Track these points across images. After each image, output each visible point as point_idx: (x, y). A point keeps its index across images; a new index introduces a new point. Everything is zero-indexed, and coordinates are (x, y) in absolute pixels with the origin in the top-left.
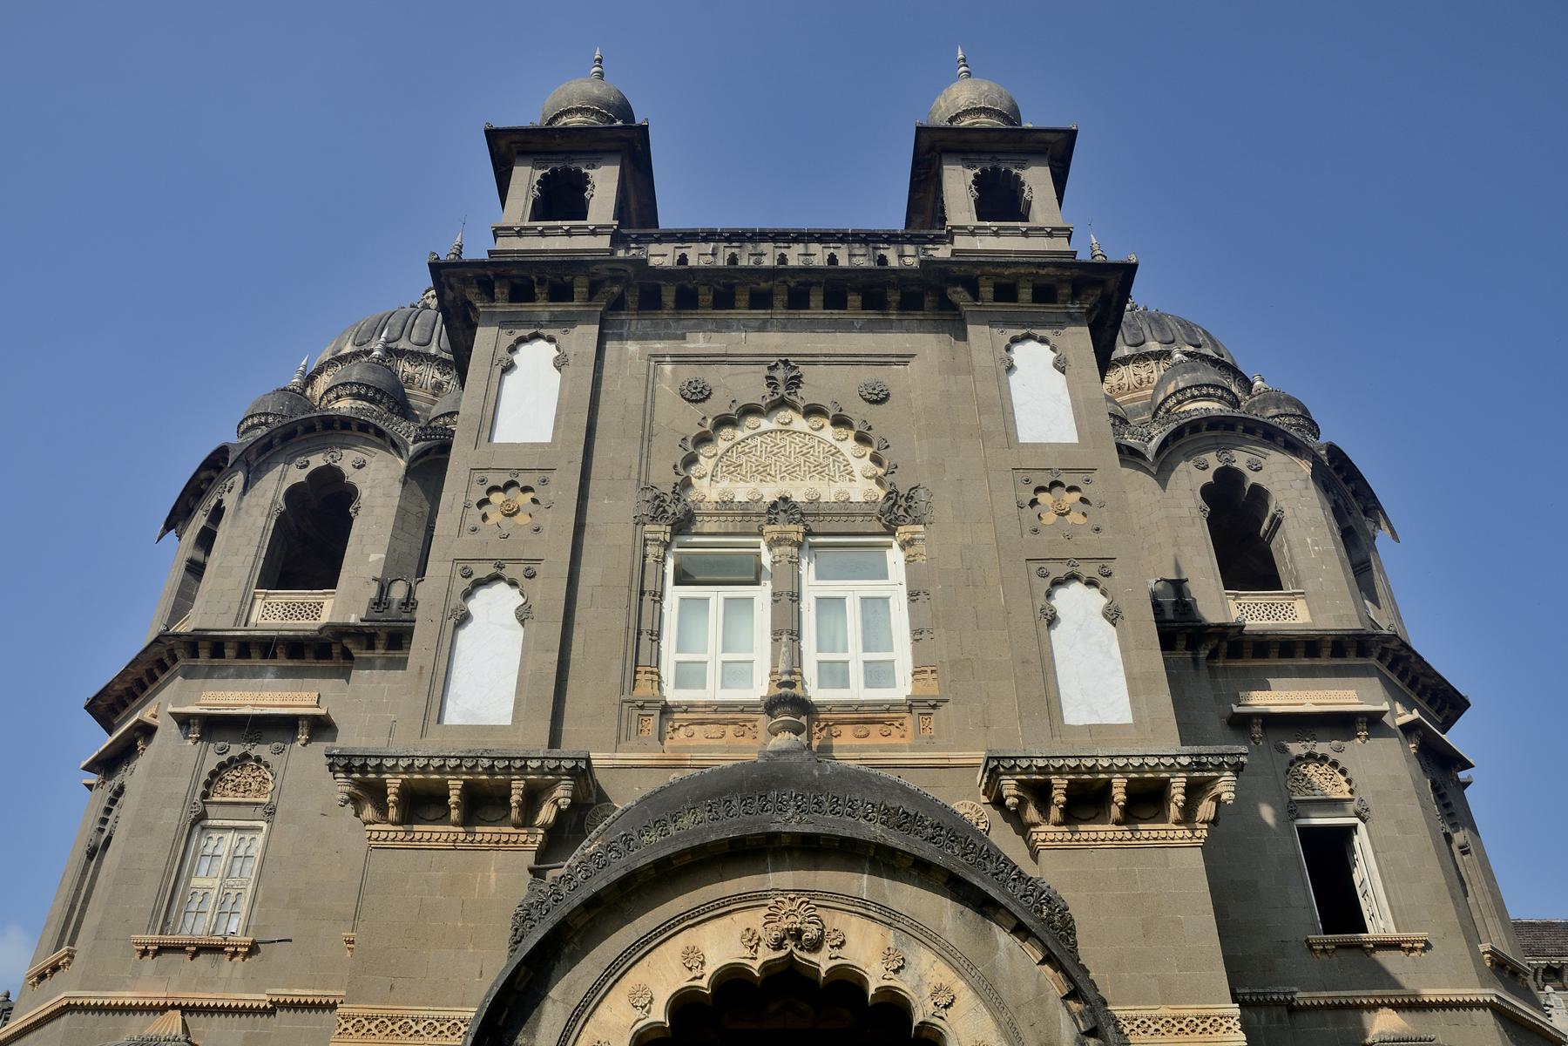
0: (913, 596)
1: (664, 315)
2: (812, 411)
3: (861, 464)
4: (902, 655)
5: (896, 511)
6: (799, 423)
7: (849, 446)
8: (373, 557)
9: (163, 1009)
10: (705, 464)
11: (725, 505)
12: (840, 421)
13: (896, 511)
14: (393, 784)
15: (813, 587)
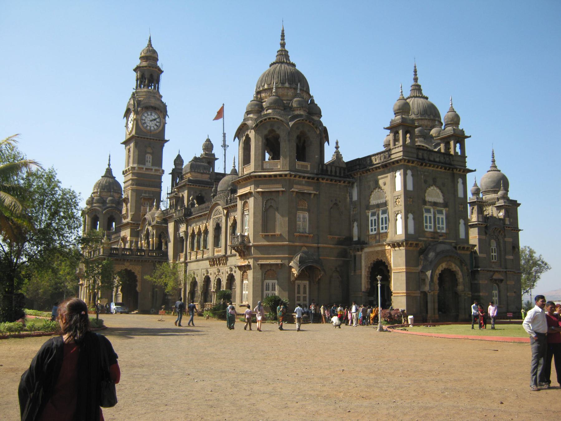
0: (446, 218)
1: (422, 167)
2: (437, 187)
3: (441, 196)
4: (444, 226)
5: (445, 205)
6: (435, 188)
7: (440, 193)
8: (316, 157)
9: (302, 246)
10: (426, 195)
11: (429, 202)
12: (440, 189)
13: (445, 205)
14: (410, 242)
15: (437, 216)
